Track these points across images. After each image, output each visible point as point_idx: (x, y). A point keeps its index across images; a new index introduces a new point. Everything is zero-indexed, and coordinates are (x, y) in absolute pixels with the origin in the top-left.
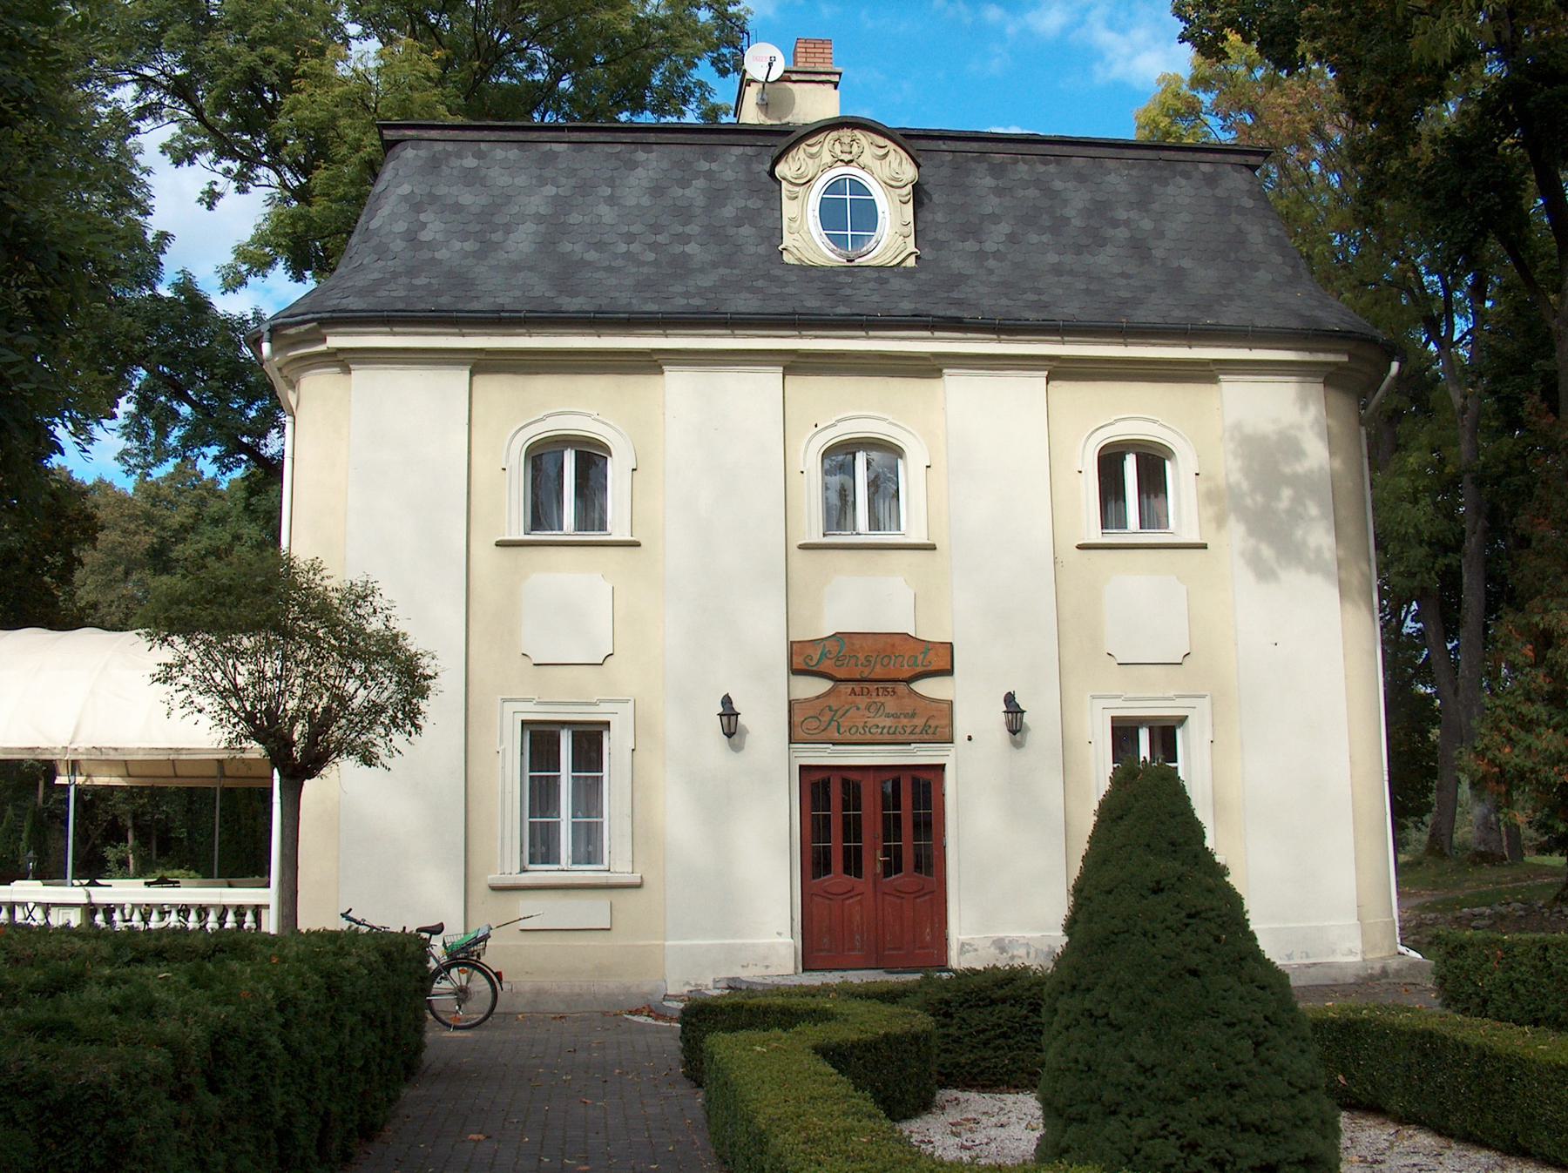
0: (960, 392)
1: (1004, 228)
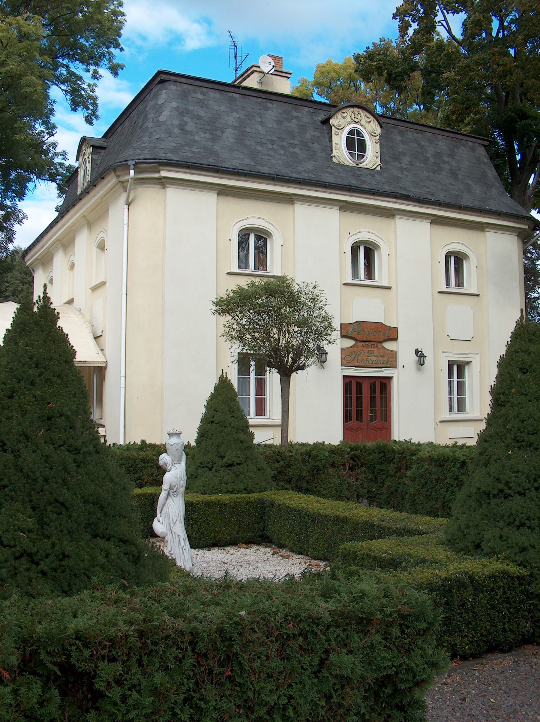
0: (402, 224)
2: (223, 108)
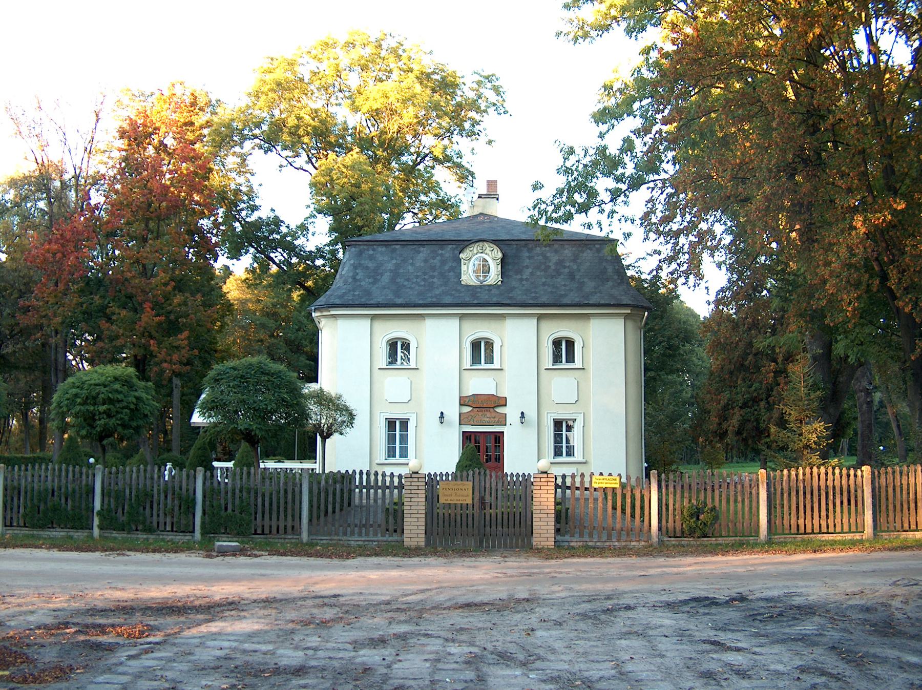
0: (510, 323)
1: (530, 270)
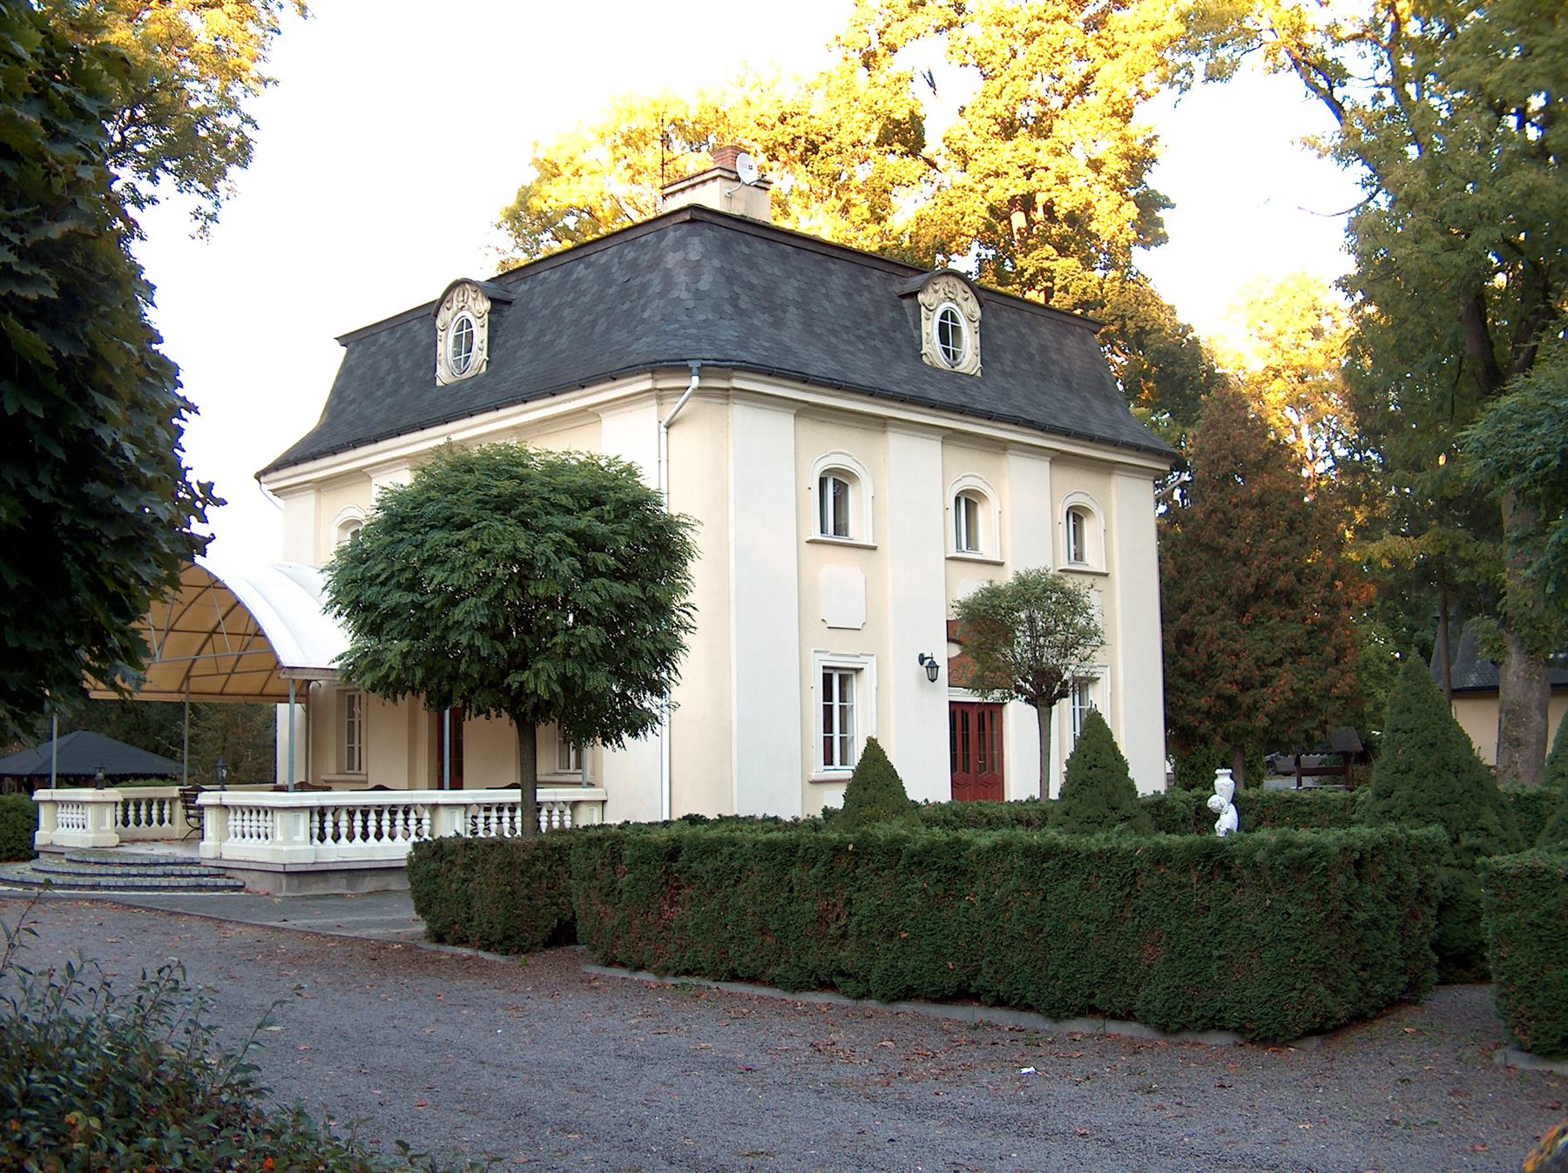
2: (777, 271)
